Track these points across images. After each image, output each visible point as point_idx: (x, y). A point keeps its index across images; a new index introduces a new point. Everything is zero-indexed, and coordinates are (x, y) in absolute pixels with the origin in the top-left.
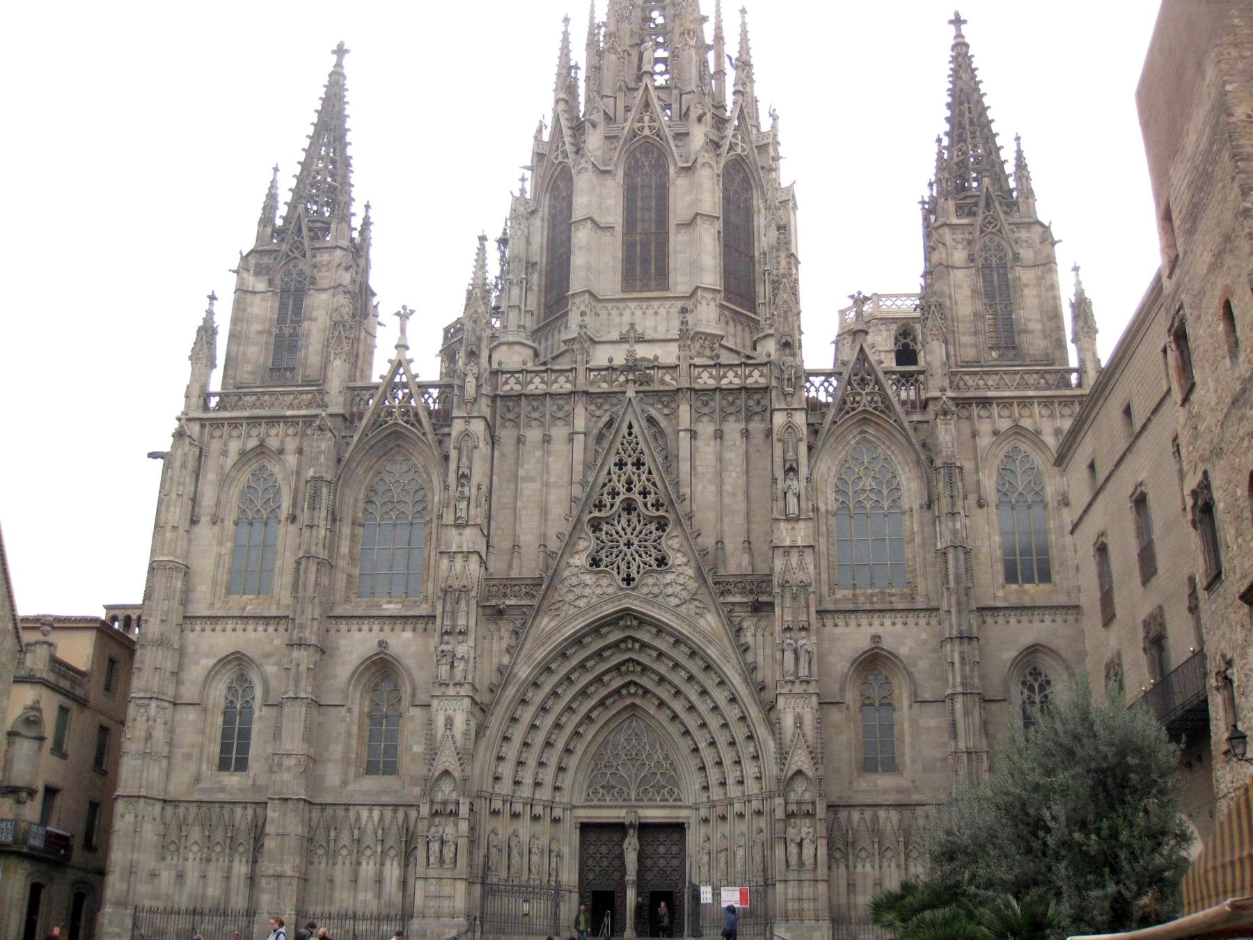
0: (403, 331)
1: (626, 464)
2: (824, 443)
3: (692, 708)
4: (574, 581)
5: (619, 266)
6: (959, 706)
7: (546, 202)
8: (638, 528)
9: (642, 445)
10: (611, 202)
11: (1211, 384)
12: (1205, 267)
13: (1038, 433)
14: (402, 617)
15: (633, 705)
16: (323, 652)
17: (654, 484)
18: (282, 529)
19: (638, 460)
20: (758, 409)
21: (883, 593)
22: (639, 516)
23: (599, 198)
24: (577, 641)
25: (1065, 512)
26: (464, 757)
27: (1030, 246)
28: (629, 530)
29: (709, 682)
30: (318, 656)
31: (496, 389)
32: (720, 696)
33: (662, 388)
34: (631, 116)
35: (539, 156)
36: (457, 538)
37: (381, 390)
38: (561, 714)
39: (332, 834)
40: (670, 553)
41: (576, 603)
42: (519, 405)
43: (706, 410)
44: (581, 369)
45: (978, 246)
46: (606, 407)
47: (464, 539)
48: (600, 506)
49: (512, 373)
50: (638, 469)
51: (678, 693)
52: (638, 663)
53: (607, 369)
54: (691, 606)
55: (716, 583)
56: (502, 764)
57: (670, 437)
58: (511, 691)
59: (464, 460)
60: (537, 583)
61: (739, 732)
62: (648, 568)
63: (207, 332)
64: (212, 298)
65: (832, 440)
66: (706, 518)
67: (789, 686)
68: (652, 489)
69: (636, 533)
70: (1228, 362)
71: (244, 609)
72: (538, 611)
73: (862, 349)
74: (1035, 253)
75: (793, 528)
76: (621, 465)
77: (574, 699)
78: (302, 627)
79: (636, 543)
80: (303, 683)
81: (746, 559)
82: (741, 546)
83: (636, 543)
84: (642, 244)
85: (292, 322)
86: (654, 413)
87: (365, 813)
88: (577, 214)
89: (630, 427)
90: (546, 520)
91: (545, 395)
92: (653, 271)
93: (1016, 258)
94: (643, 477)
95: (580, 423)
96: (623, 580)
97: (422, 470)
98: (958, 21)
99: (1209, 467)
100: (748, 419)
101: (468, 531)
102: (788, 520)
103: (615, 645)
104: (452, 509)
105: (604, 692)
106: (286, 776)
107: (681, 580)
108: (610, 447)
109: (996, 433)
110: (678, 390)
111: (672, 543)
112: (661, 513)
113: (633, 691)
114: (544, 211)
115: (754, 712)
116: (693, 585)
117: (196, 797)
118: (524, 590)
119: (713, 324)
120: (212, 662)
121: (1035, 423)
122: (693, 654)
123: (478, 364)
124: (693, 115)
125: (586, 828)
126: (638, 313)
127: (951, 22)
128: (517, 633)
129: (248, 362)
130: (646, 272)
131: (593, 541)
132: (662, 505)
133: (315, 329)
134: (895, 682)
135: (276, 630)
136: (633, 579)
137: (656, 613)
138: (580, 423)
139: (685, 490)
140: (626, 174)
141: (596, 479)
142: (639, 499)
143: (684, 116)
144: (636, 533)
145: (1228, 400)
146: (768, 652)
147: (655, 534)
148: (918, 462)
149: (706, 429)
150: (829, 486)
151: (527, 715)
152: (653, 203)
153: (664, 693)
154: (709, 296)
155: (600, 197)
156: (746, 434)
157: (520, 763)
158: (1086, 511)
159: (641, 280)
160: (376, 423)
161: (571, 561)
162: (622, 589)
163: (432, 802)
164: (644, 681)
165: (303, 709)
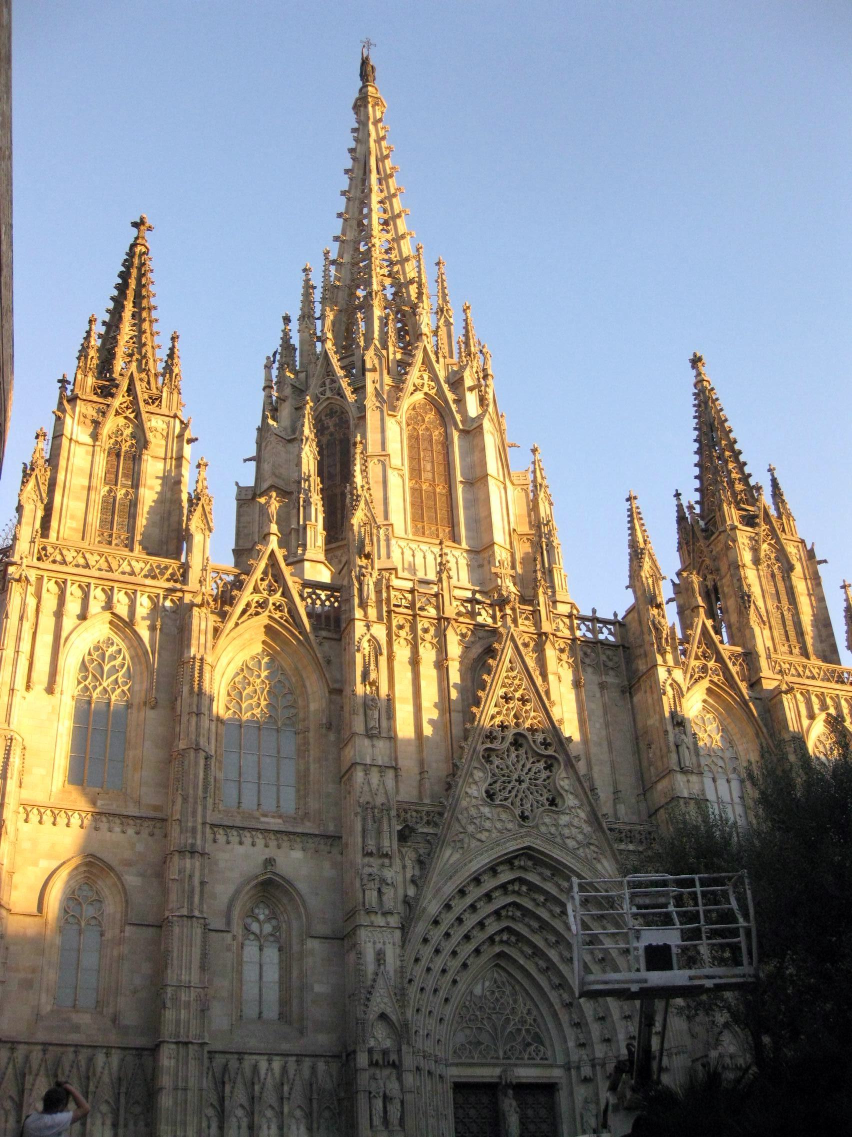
4: (473, 812)
8: (528, 766)
22: (526, 753)
36: (370, 750)
39: (228, 1088)
41: (479, 836)
45: (762, 554)
47: (377, 751)
50: (524, 704)
55: (610, 830)
75: (688, 781)
76: (507, 698)
78: (194, 830)
80: (196, 899)
82: (612, 796)
87: (263, 1065)
89: (510, 662)
98: (696, 361)
101: (381, 744)
102: (683, 771)
103: (504, 887)
104: (361, 718)
106: (183, 1014)
107: (576, 822)
109: (812, 717)
112: (550, 752)
113: (505, 938)
116: (587, 829)
117: (41, 1036)
118: (425, 819)
120: (55, 864)
125: (460, 1087)
128: (421, 863)
129: (73, 517)
132: (550, 744)
137: (556, 853)
138: (454, 649)
140: (408, 425)
143: (456, 383)
144: (526, 770)
147: (544, 775)
149: (568, 675)
161: (468, 790)
162: (521, 826)
163: (370, 1051)
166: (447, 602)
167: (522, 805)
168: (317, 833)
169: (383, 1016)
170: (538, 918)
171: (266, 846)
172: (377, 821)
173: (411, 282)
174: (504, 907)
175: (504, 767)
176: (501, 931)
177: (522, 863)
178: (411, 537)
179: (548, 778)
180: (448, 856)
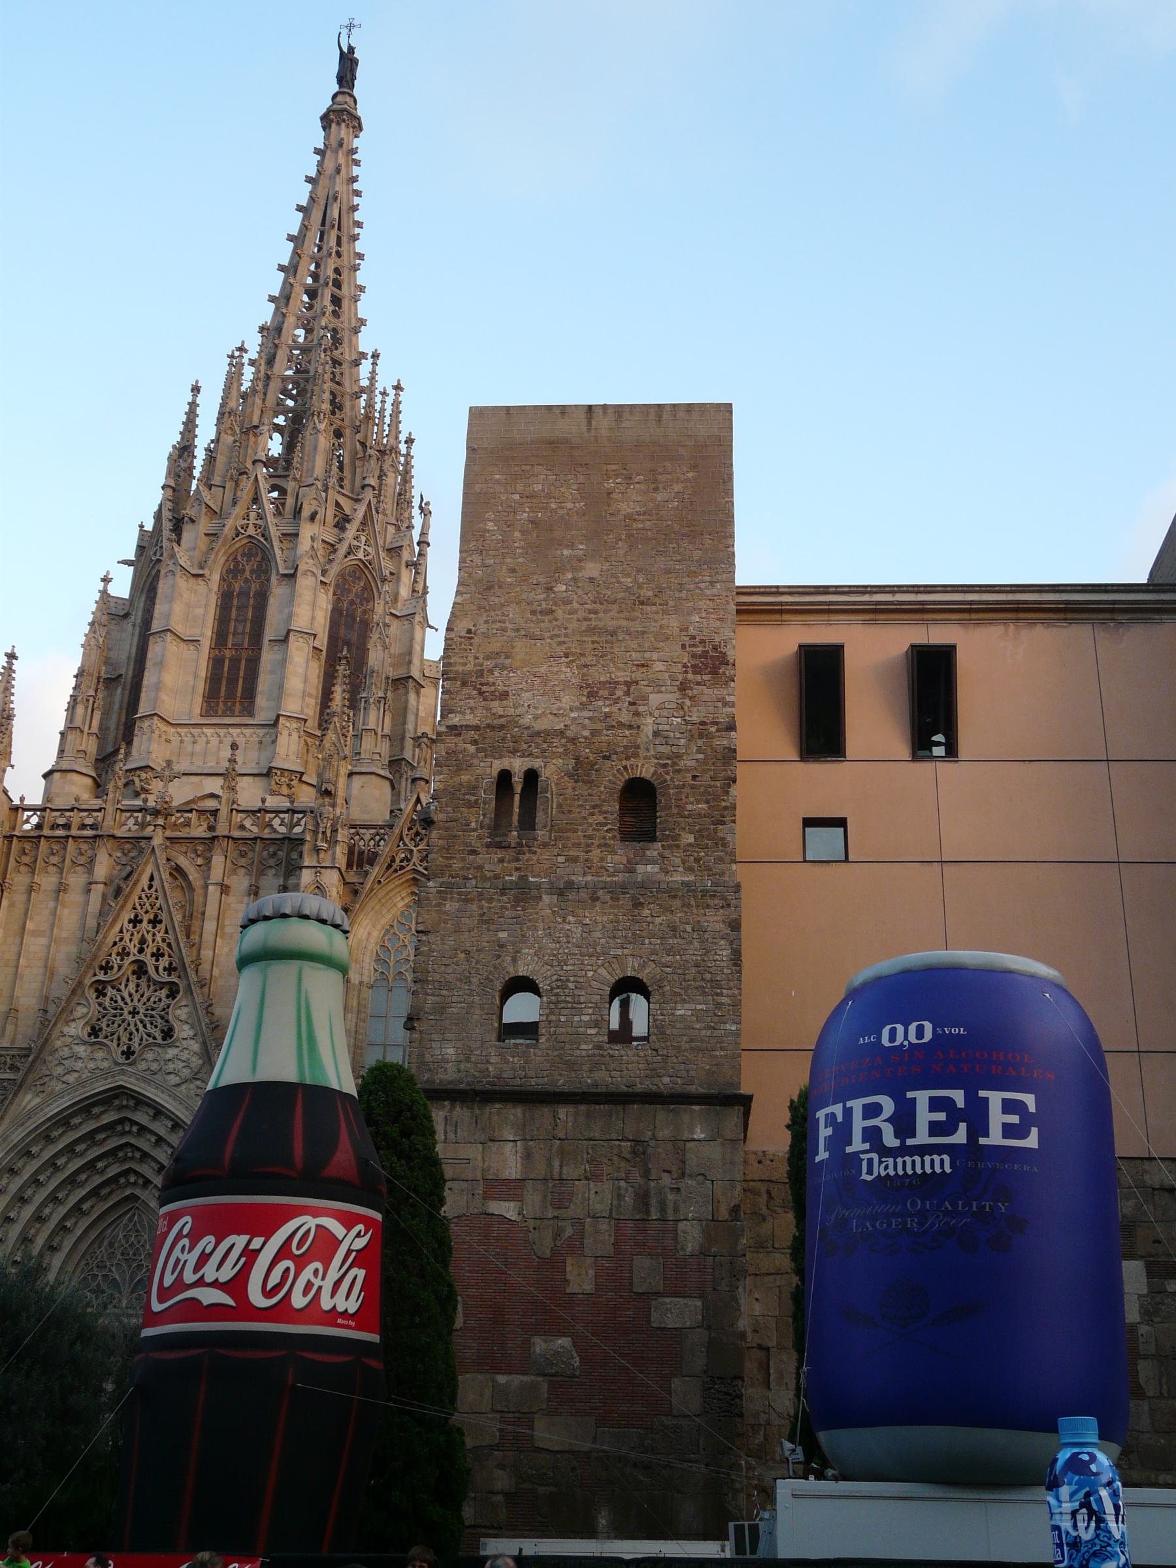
1: (141, 921)
2: (362, 907)
4: (66, 1052)
5: (201, 686)
10: (199, 611)
15: (133, 1197)
17: (169, 945)
19: (156, 916)
22: (149, 980)
24: (63, 1121)
28: (136, 997)
31: (14, 828)
34: (239, 510)
38: (43, 1205)
41: (64, 1079)
42: (38, 847)
43: (243, 861)
44: (110, 809)
46: (132, 854)
48: (106, 968)
49: (34, 809)
50: (154, 927)
52: (138, 1149)
54: (192, 1086)
57: (199, 891)
60: (25, 1053)
62: (151, 1040)
65: (375, 900)
69: (144, 999)
72: (21, 1086)
76: (136, 921)
79: (142, 1011)
83: (142, 1011)
84: (230, 660)
86: (183, 862)
89: (152, 879)
90: (51, 980)
91: (67, 837)
92: (239, 693)
94: (159, 938)
96: (123, 1053)
103: (110, 1126)
105: (98, 1180)
107: (185, 1055)
108: (126, 901)
110: (214, 838)
111: (180, 1013)
112: (173, 979)
113: (132, 1180)
114: (137, 616)
119: (293, 758)
124: (306, 513)
126: (214, 741)
130: (231, 694)
131: (94, 1006)
132: (175, 969)
136: (133, 1053)
137: (151, 1093)
139: (206, 954)
140: (223, 579)
141: (105, 937)
143: (297, 512)
144: (144, 999)
147: (165, 1001)
149: (240, 882)
150: (369, 953)
154: (295, 725)
155: (188, 605)
159: (225, 703)
161: (66, 1030)
166: (109, 817)
167: (130, 1040)
175: (119, 999)
177: (125, 1103)
180: (28, 1100)
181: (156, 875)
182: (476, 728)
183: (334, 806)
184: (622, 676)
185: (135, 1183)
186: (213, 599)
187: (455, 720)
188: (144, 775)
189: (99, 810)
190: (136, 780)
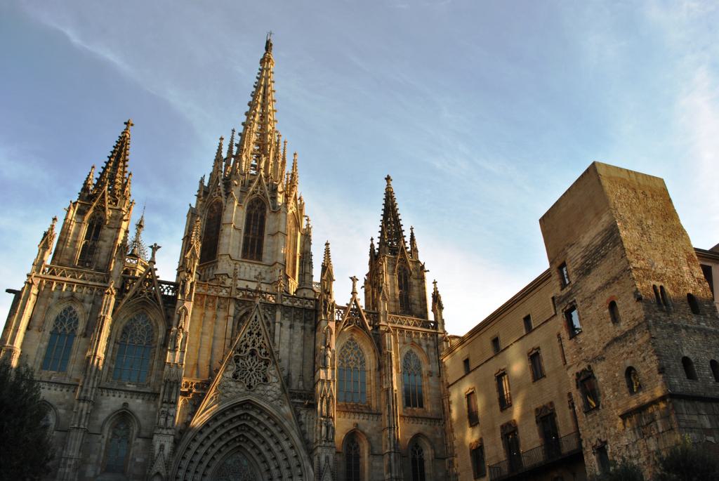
0: (153, 255)
3: (270, 450)
5: (241, 247)
6: (392, 457)
7: (207, 212)
8: (256, 363)
9: (261, 326)
11: (596, 333)
12: (595, 288)
13: (420, 345)
14: (136, 392)
16: (94, 404)
17: (265, 344)
18: (77, 340)
20: (309, 318)
21: (357, 405)
23: (235, 214)
25: (430, 379)
26: (167, 465)
27: (417, 270)
29: (281, 438)
30: (91, 408)
32: (286, 445)
33: (267, 302)
34: (254, 185)
35: (204, 192)
37: (140, 281)
40: (270, 376)
41: (226, 395)
43: (287, 315)
44: (234, 288)
48: (240, 351)
51: (264, 442)
52: (247, 426)
53: (245, 290)
56: (180, 471)
57: (272, 325)
58: (190, 435)
59: (182, 321)
61: (294, 463)
63: (47, 237)
64: (55, 219)
66: (285, 363)
67: (323, 443)
68: (264, 346)
70: (611, 325)
71: (50, 378)
73: (355, 301)
74: (418, 274)
76: (251, 333)
77: (215, 441)
78: (87, 391)
79: (254, 370)
80: (83, 420)
81: (301, 383)
85: (93, 240)
88: (225, 219)
89: (256, 317)
93: (411, 273)
94: (261, 341)
95: (232, 311)
97: (153, 321)
98: (388, 179)
99: (591, 364)
100: (305, 322)
103: (239, 417)
104: (173, 342)
105: (229, 439)
107: (274, 389)
111: (272, 371)
112: (267, 358)
113: (241, 439)
115: (303, 454)
116: (279, 392)
121: (419, 341)
122: (275, 424)
123: (192, 277)
126: (248, 268)
127: (386, 179)
130: (252, 251)
133: (104, 245)
134: (361, 445)
135: (68, 391)
137: (262, 403)
140: (248, 209)
142: (258, 350)
145: (610, 339)
146: (311, 427)
148: (374, 351)
149: (287, 323)
151: (194, 446)
152: (258, 223)
153: (256, 441)
156: (304, 328)
157: (188, 471)
158: (460, 379)
160: (134, 296)
164: (248, 435)
165: (82, 434)
168: (149, 391)
169: (158, 474)
170: (255, 431)
171: (126, 397)
172: (171, 388)
173: (269, 143)
174: (239, 426)
176: (239, 436)
178: (240, 259)
179: (265, 369)
181: (258, 316)
182: (641, 268)
183: (331, 298)
184: (673, 259)
185: (243, 441)
186: (245, 215)
187: (634, 265)
188: (224, 277)
189: (229, 288)
190: (220, 278)
